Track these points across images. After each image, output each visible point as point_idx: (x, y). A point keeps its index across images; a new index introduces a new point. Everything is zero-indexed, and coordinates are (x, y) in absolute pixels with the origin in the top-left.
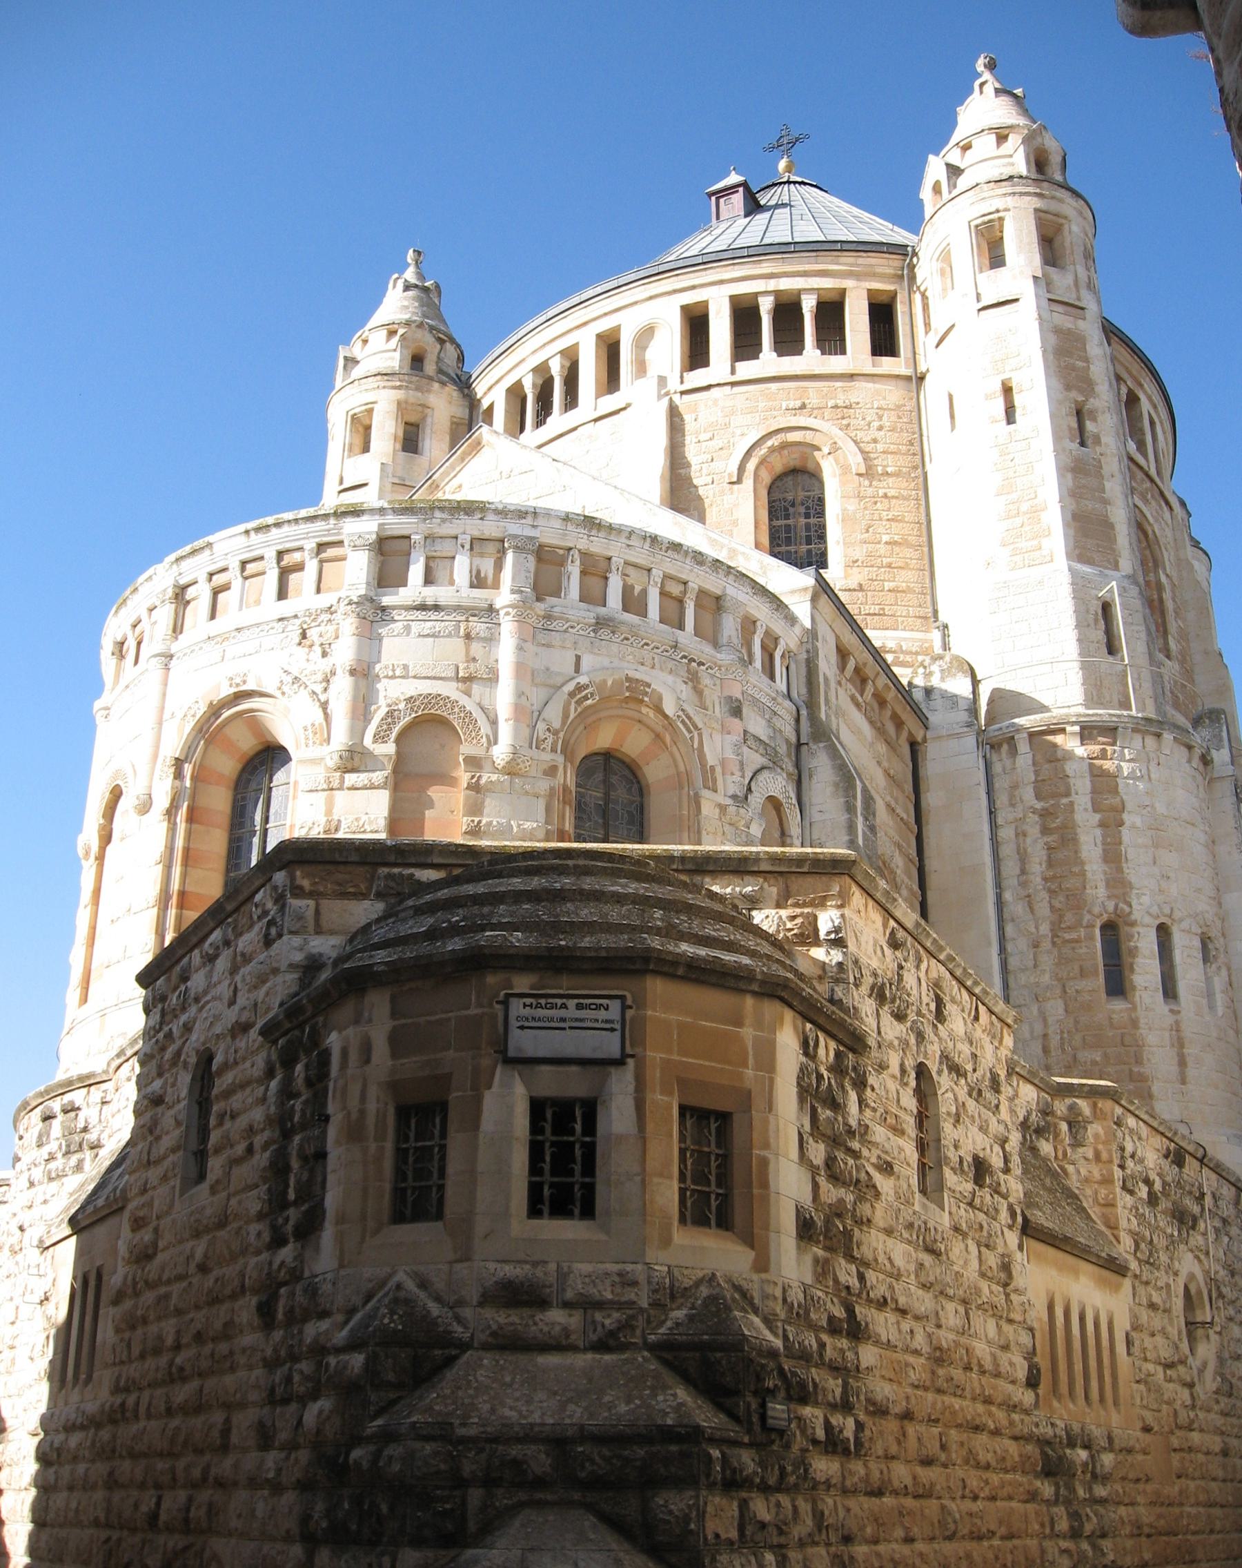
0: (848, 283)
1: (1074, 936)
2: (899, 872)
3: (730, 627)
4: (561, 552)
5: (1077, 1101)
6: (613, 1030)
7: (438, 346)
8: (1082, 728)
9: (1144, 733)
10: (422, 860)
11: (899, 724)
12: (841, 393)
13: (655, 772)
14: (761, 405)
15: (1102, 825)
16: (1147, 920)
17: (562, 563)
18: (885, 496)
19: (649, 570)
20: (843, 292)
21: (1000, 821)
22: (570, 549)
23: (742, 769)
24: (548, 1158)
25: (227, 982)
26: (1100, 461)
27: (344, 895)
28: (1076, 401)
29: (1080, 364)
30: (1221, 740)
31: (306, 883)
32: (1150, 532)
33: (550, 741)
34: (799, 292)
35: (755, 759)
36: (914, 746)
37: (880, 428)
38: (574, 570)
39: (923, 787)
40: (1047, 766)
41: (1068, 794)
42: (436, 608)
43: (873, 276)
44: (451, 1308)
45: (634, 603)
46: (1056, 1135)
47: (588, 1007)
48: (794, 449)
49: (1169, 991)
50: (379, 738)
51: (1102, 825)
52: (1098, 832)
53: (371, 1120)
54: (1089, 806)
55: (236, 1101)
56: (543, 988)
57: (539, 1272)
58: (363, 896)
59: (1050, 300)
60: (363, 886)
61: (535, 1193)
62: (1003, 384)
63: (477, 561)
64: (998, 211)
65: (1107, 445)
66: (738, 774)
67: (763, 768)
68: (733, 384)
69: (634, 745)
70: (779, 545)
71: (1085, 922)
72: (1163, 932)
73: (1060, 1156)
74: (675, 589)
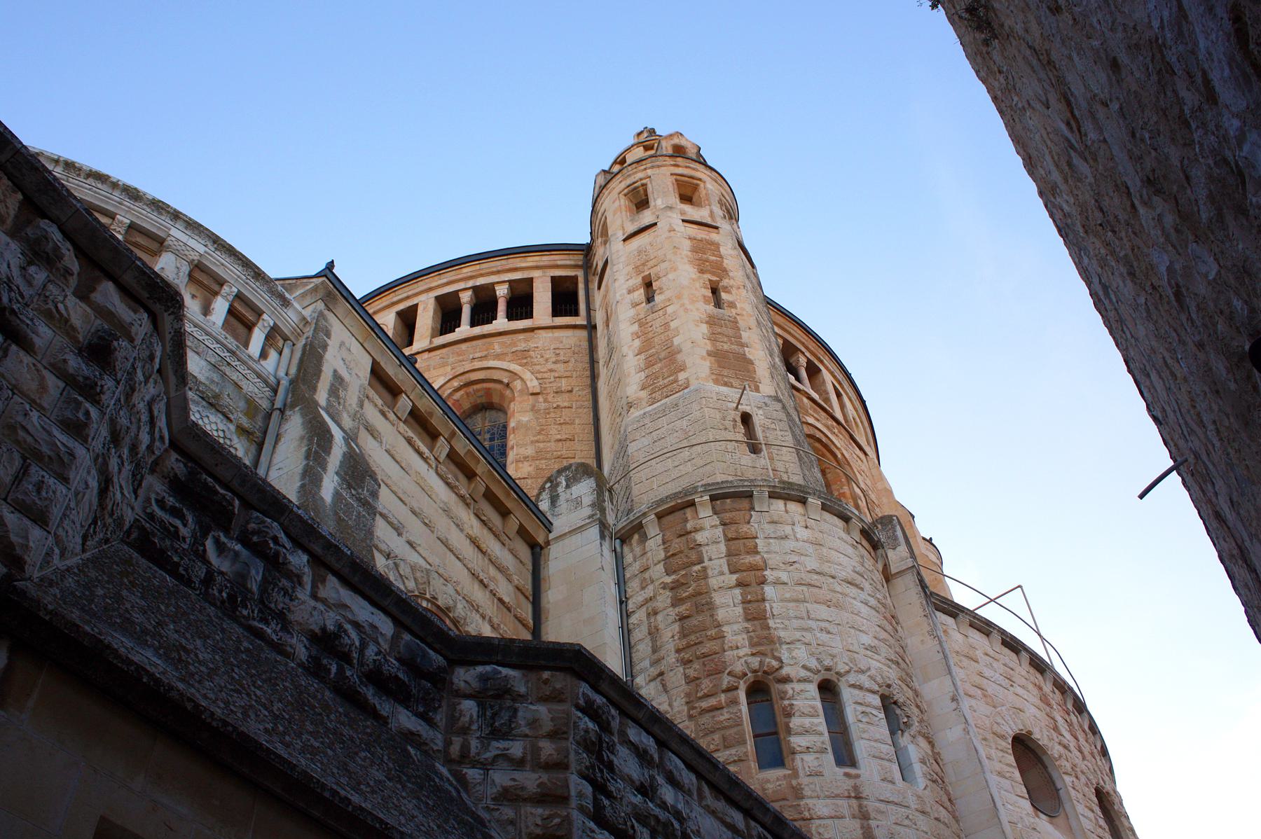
0: (535, 274)
1: (712, 702)
5: (505, 671)
8: (713, 498)
9: (787, 498)
11: (504, 513)
12: (521, 342)
14: (451, 360)
15: (740, 584)
16: (803, 673)
18: (558, 406)
20: (530, 281)
26: (735, 318)
28: (710, 280)
30: (896, 539)
32: (839, 456)
34: (493, 284)
36: (537, 550)
37: (555, 363)
39: (544, 586)
40: (678, 540)
41: (701, 561)
43: (557, 267)
46: (453, 718)
48: (476, 387)
49: (845, 755)
51: (740, 584)
52: (737, 591)
54: (726, 569)
59: (683, 221)
62: (643, 278)
64: (641, 179)
65: (743, 309)
68: (430, 350)
71: (724, 687)
72: (828, 689)
73: (455, 749)
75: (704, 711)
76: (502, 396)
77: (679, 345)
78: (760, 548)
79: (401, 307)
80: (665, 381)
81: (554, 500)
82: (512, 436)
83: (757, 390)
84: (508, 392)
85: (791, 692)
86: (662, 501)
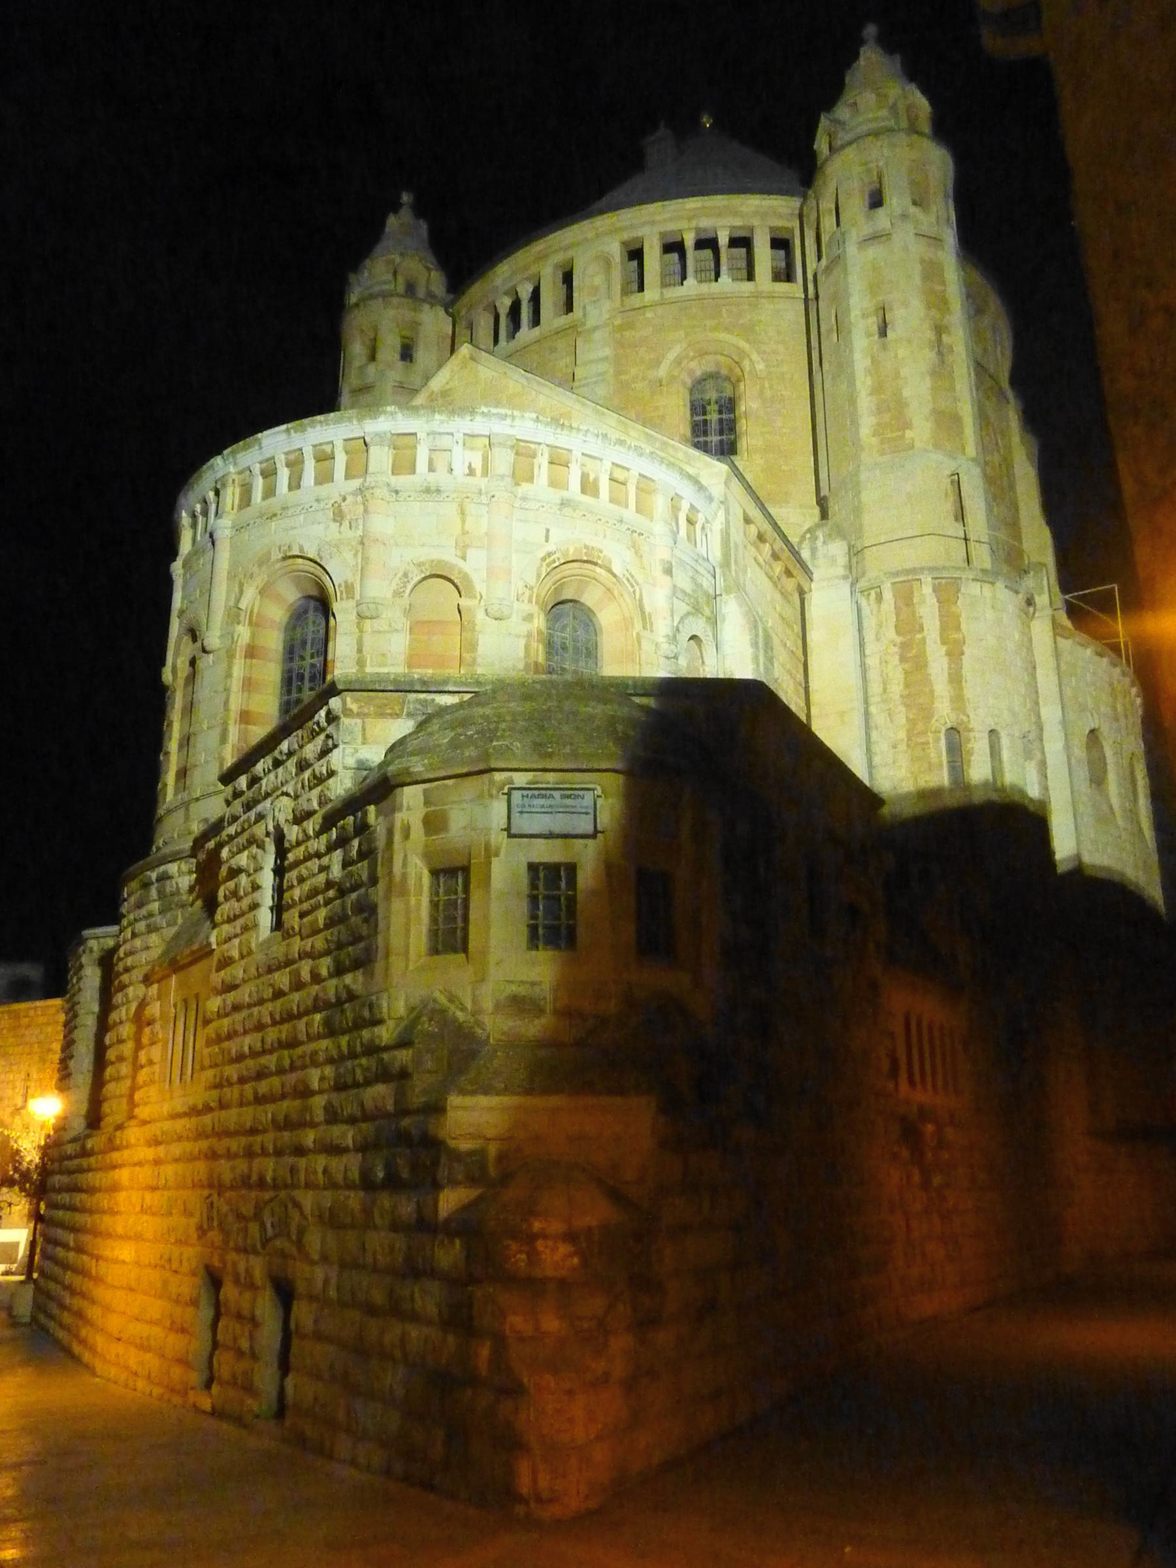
2: (789, 692)
3: (660, 504)
4: (533, 446)
6: (587, 813)
7: (427, 274)
10: (441, 689)
13: (607, 617)
17: (534, 456)
19: (601, 460)
20: (752, 229)
21: (867, 652)
22: (540, 444)
23: (672, 615)
24: (541, 907)
25: (293, 783)
27: (382, 715)
29: (938, 288)
30: (1042, 588)
31: (354, 707)
33: (528, 593)
35: (683, 608)
38: (543, 460)
41: (922, 629)
42: (438, 491)
44: (473, 1016)
45: (588, 486)
47: (569, 797)
50: (398, 594)
51: (949, 654)
53: (412, 882)
55: (303, 870)
56: (537, 783)
57: (537, 989)
58: (398, 716)
59: (916, 234)
60: (396, 708)
61: (533, 930)
63: (468, 453)
66: (669, 618)
67: (688, 614)
69: (589, 598)
70: (698, 436)
74: (620, 475)
75: (917, 744)
76: (731, 370)
77: (906, 398)
78: (963, 626)
79: (626, 236)
80: (894, 435)
81: (814, 551)
82: (744, 421)
83: (964, 454)
84: (738, 370)
85: (973, 740)
86: (897, 574)
